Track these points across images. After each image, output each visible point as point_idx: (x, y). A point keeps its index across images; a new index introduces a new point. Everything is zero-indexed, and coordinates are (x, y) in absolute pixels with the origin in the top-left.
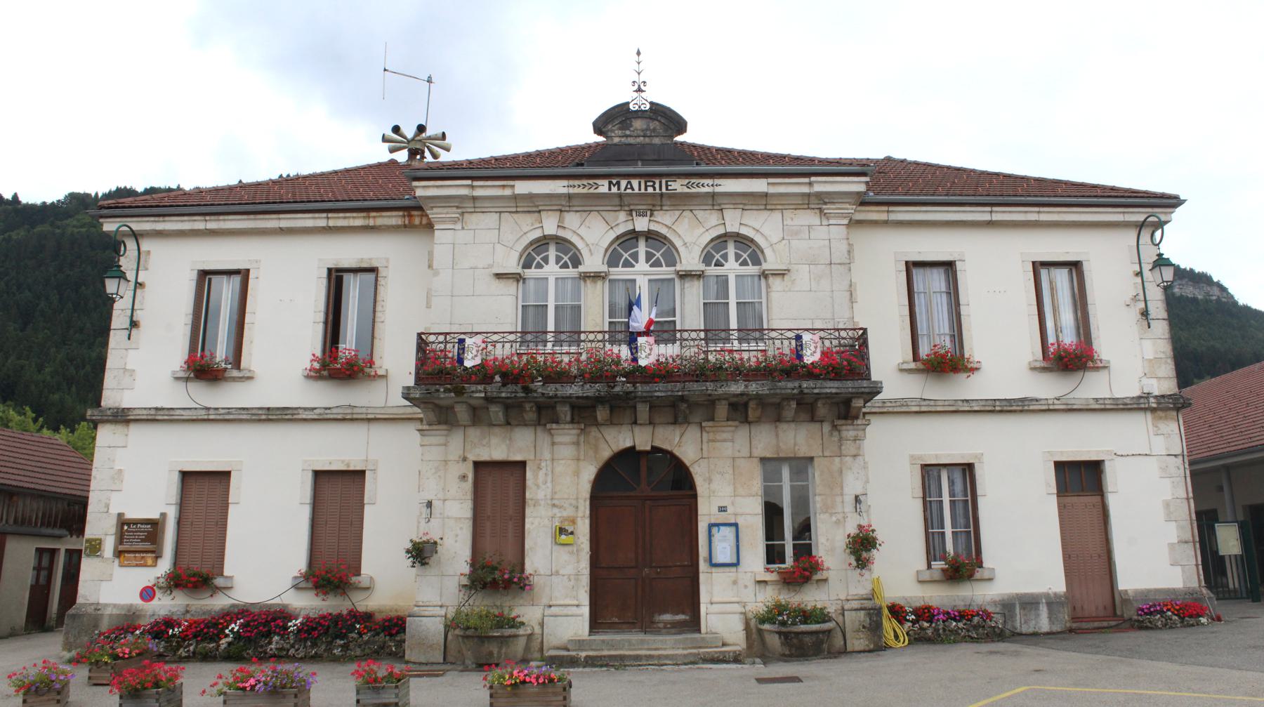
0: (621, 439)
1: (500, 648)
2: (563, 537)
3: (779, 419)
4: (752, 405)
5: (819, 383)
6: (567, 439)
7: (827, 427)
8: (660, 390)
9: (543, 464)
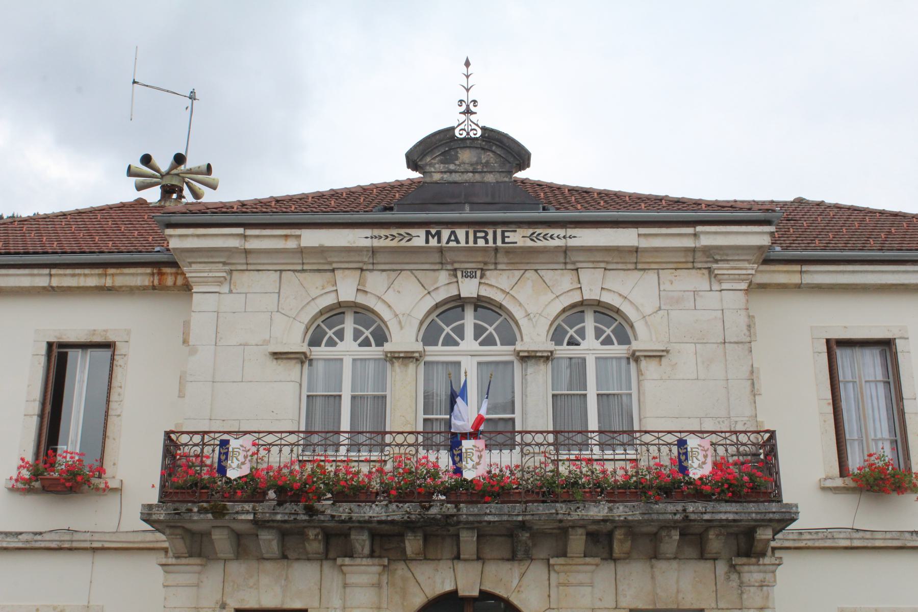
3: (655, 556)
4: (618, 535)
5: (710, 506)
6: (364, 579)
8: (492, 512)
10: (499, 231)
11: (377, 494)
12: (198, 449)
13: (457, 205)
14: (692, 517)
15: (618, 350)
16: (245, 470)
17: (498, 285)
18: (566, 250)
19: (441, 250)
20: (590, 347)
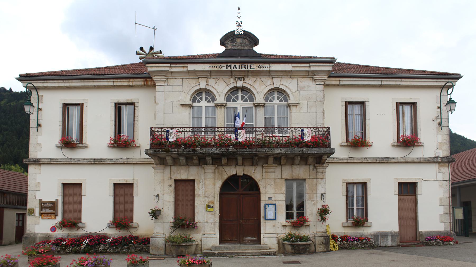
0: (231, 171)
1: (186, 250)
2: (209, 208)
3: (293, 164)
4: (283, 158)
5: (310, 149)
6: (210, 171)
7: (312, 167)
8: (247, 151)
9: (201, 181)
10: (249, 65)
11: (213, 146)
12: (160, 133)
13: (236, 57)
14: (305, 152)
15: (284, 103)
16: (175, 139)
17: (249, 83)
18: (269, 71)
19: (231, 71)
20: (276, 102)
